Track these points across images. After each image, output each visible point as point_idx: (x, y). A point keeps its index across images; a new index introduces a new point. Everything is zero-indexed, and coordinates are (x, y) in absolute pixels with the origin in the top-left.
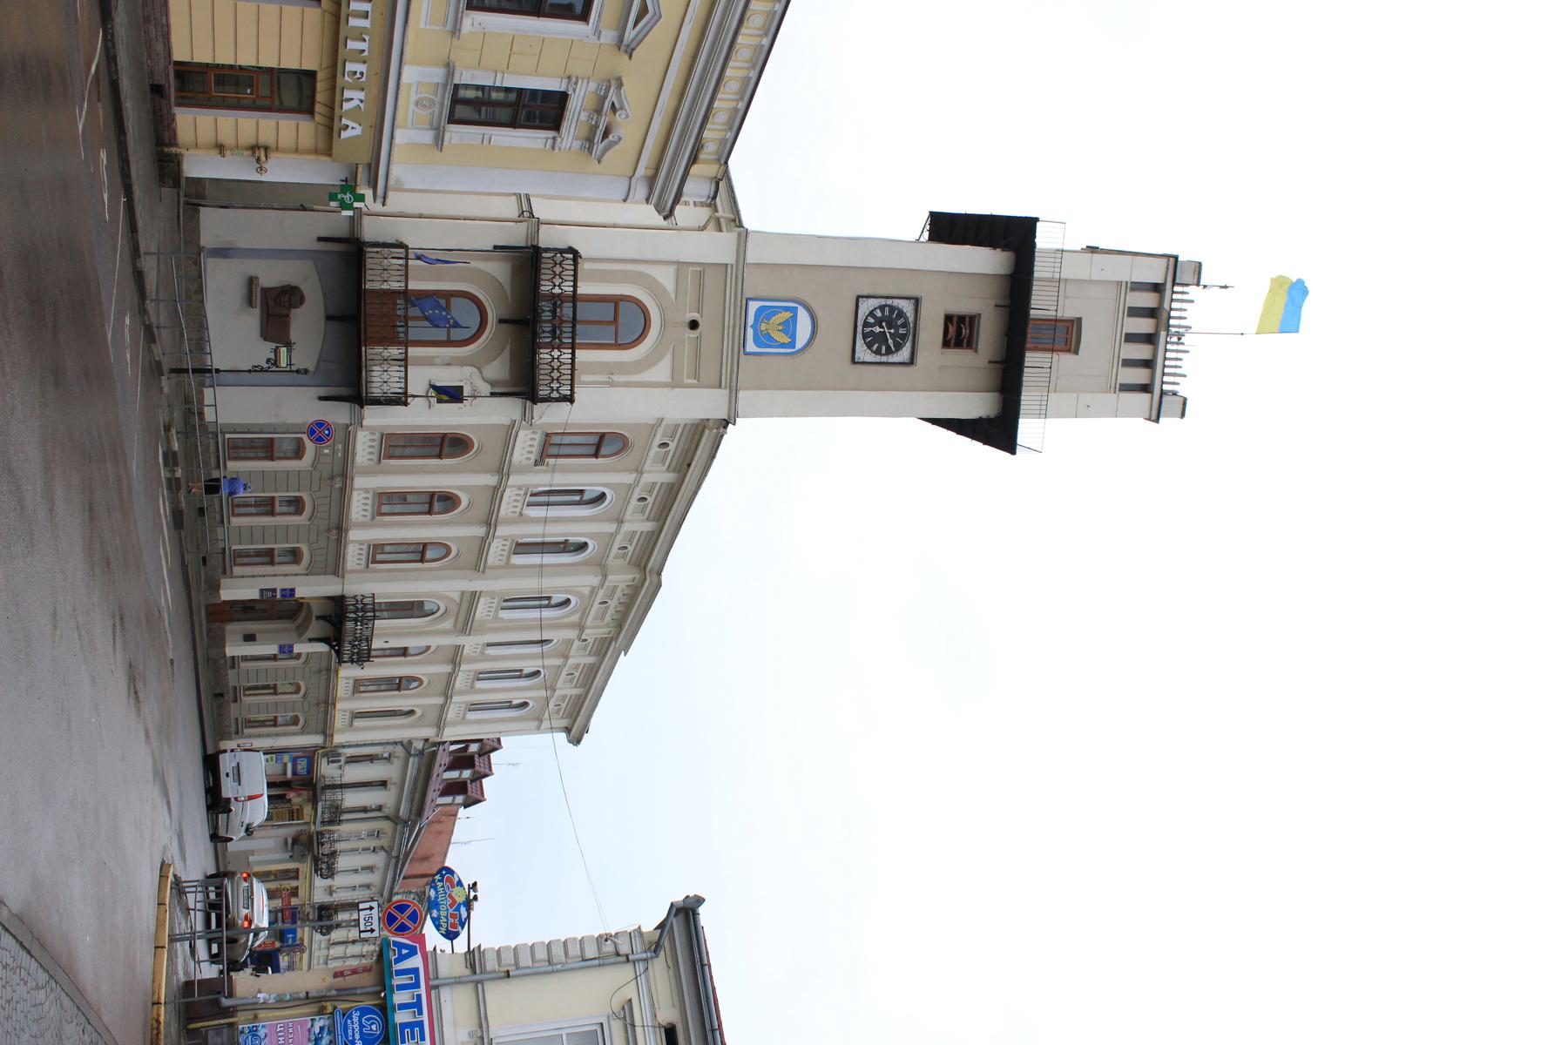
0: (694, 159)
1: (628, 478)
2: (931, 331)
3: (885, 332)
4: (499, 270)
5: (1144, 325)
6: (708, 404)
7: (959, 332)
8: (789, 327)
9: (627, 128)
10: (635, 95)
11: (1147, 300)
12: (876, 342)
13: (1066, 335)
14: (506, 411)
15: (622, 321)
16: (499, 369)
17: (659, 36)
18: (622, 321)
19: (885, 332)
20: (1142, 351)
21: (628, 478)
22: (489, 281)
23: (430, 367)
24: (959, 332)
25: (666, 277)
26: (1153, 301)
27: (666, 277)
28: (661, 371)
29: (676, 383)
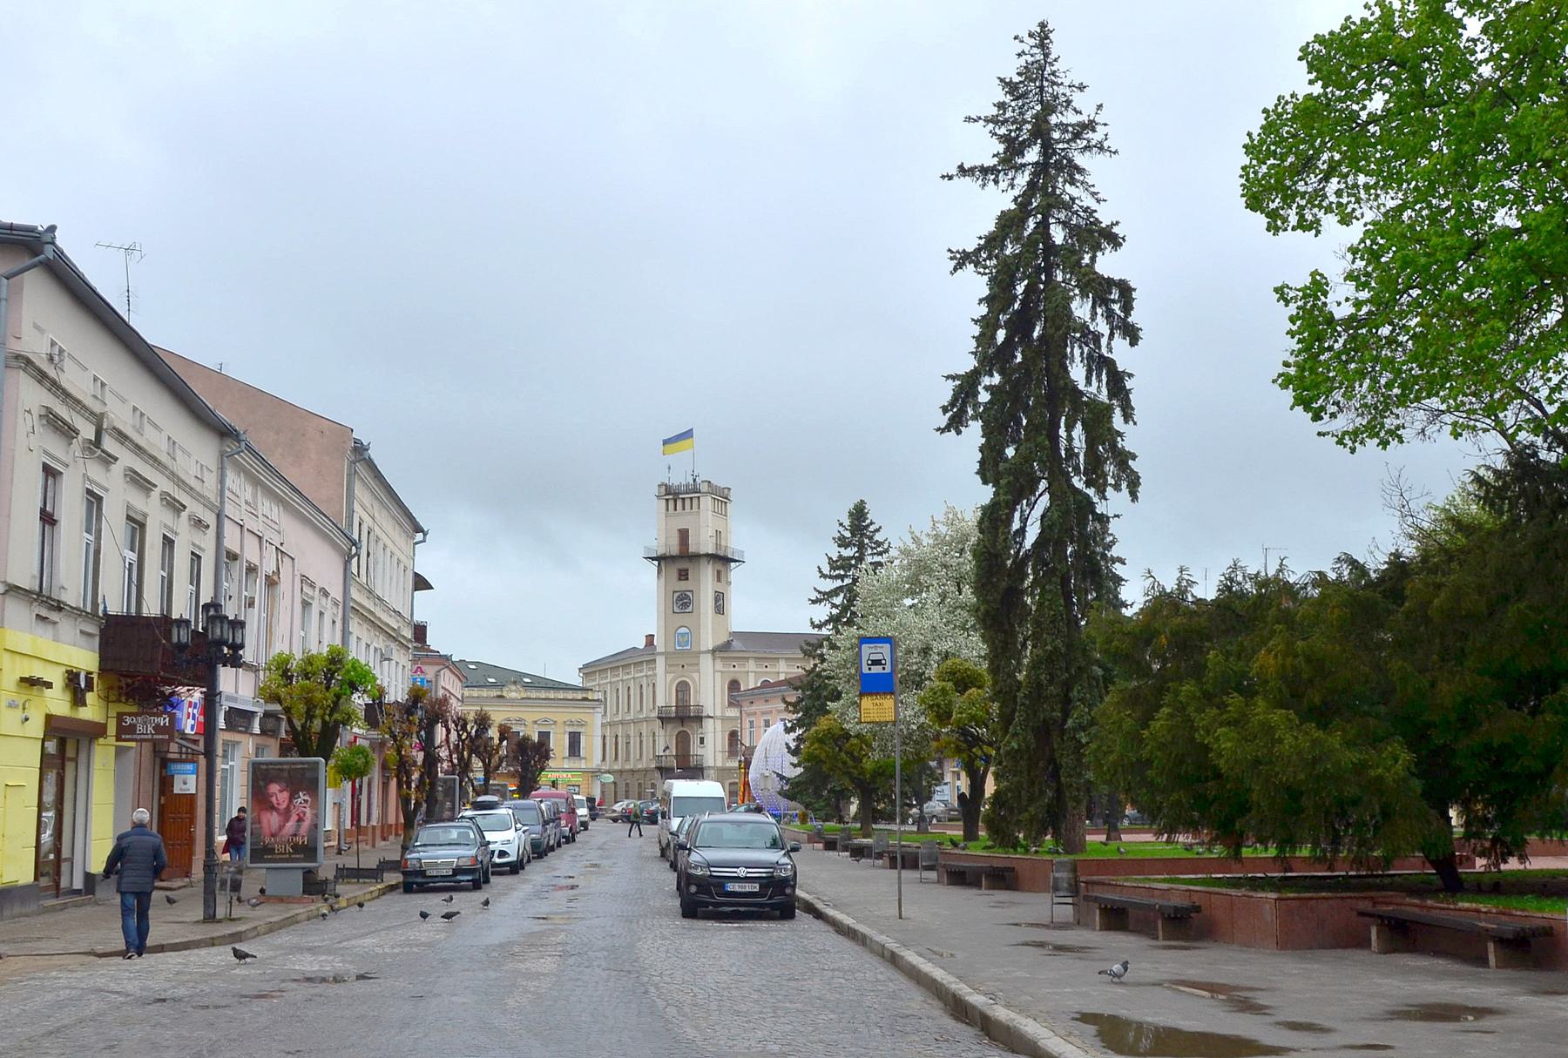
0: (585, 699)
1: (752, 676)
2: (683, 585)
3: (683, 602)
4: (669, 727)
5: (679, 503)
6: (706, 663)
7: (683, 575)
8: (683, 635)
9: (575, 718)
10: (566, 718)
11: (671, 504)
12: (685, 605)
13: (684, 535)
14: (708, 724)
15: (683, 688)
16: (695, 725)
17: (550, 716)
18: (683, 688)
19: (683, 602)
20: (688, 502)
21: (752, 676)
22: (674, 730)
23: (695, 749)
24: (683, 575)
25: (670, 677)
26: (673, 496)
27: (670, 677)
28: (695, 675)
29: (698, 671)
